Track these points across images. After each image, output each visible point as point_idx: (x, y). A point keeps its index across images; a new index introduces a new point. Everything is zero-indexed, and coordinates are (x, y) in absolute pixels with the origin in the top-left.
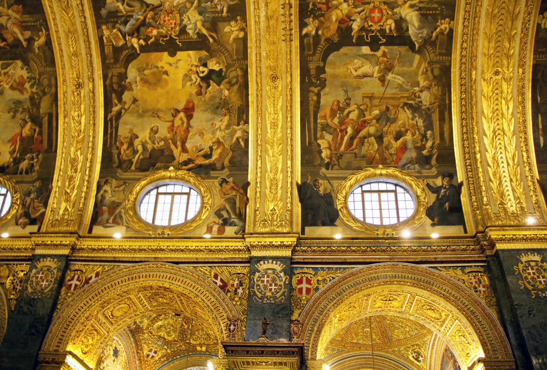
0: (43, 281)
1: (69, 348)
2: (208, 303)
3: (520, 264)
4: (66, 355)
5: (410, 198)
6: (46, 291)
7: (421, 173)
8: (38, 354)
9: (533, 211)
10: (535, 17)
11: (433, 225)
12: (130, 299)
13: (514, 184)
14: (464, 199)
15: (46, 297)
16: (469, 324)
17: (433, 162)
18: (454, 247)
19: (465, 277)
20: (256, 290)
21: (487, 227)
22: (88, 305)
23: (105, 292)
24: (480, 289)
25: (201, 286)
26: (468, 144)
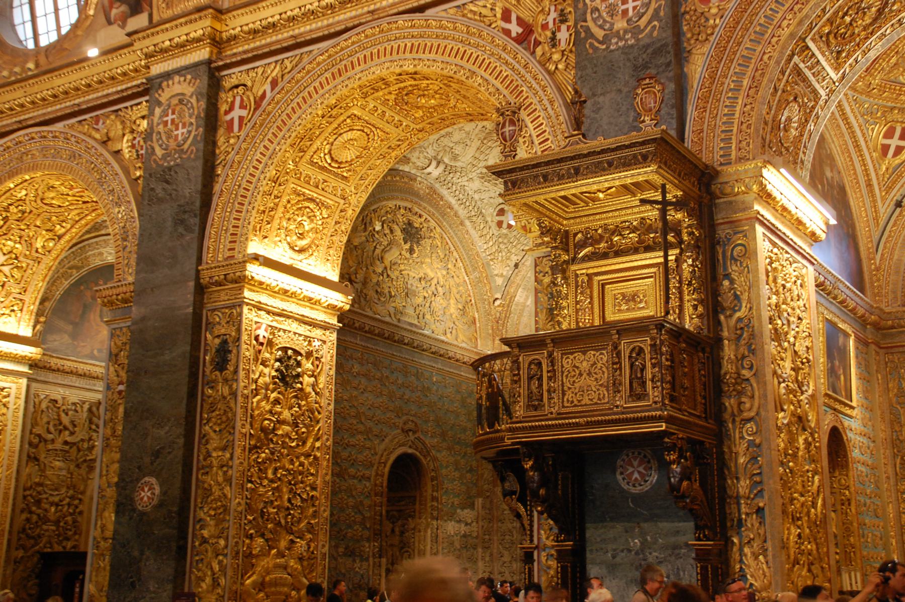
0: (177, 129)
1: (254, 247)
2: (497, 83)
4: (245, 262)
6: (186, 147)
8: (198, 272)
12: (353, 117)
15: (189, 158)
20: (590, 24)
22: (268, 153)
23: (294, 117)
25: (477, 46)
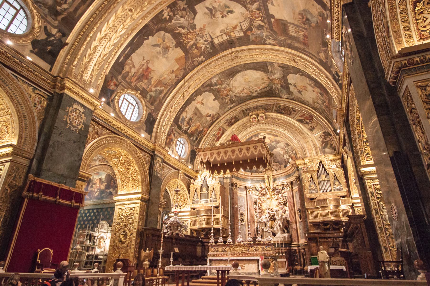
3: (71, 107)
5: (26, 24)
7: (46, 17)
9: (95, 87)
10: (165, 6)
11: (32, 52)
13: (95, 67)
14: (63, 53)
16: (18, 122)
17: (60, 18)
18: (38, 74)
19: (33, 95)
21: (67, 78)
24: (38, 106)
26: (88, 28)
